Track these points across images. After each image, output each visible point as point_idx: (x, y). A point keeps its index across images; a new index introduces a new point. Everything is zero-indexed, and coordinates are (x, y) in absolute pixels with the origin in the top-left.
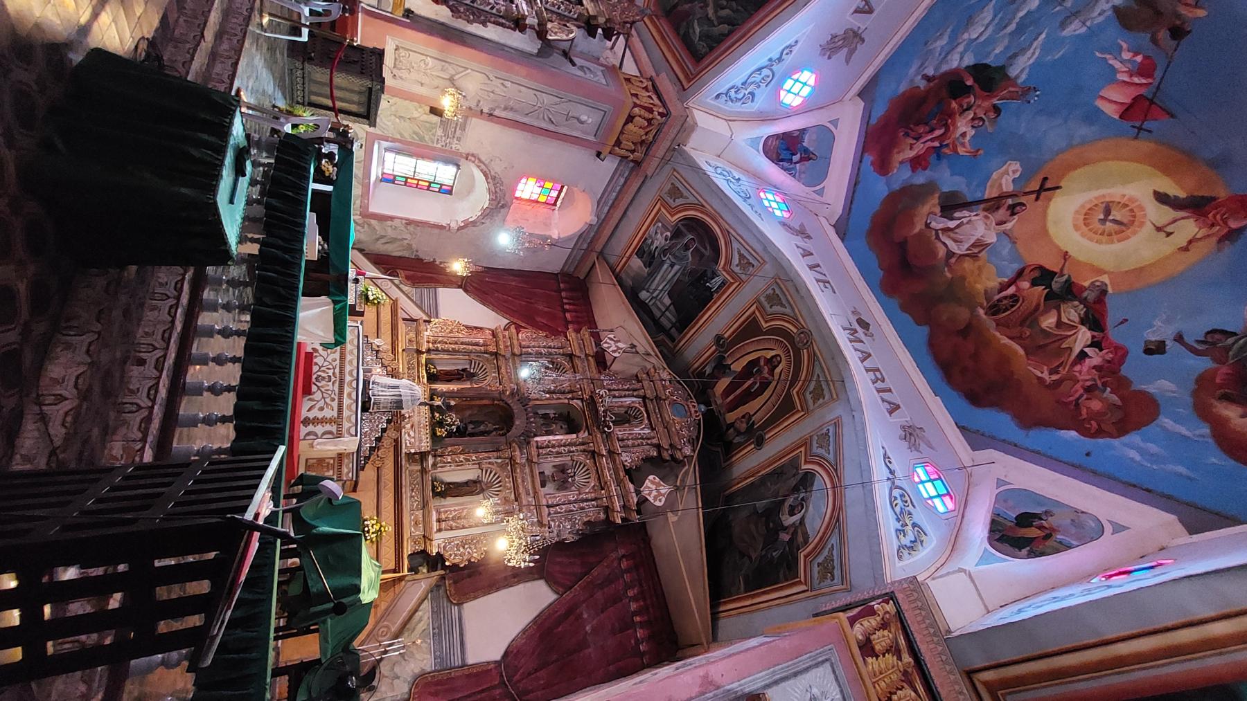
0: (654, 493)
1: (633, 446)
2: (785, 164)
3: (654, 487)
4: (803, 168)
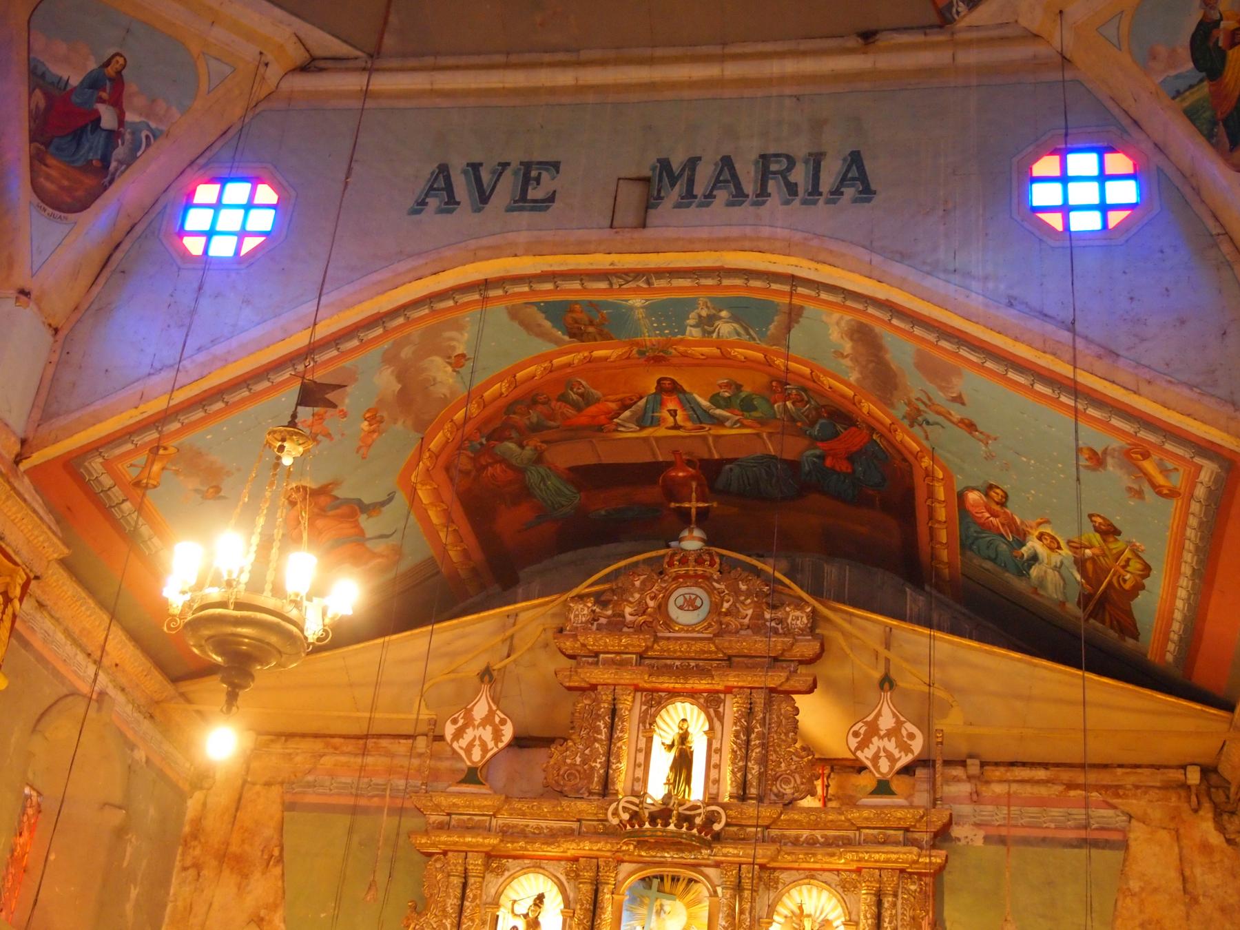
0: (891, 745)
2: (120, 152)
4: (139, 101)
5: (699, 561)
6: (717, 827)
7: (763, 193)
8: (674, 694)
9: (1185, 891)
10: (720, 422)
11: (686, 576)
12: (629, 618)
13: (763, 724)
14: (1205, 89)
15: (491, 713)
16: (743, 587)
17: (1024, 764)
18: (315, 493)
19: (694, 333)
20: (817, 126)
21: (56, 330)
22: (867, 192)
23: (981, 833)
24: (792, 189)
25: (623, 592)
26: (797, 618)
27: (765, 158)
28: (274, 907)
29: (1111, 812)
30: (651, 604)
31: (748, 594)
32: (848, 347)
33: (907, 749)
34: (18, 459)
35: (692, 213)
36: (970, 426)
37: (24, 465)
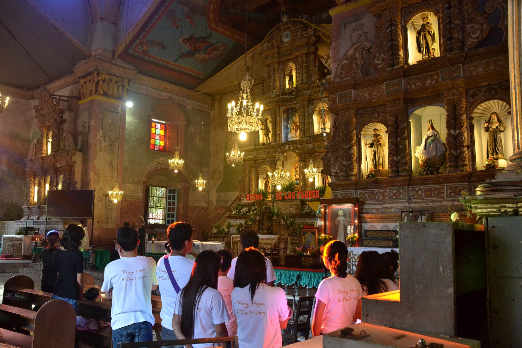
5: (287, 24)
8: (289, 60)
11: (285, 29)
13: (306, 62)
15: (249, 78)
18: (188, 40)
21: (115, 24)
26: (310, 31)
34: (113, 56)
37: (116, 57)
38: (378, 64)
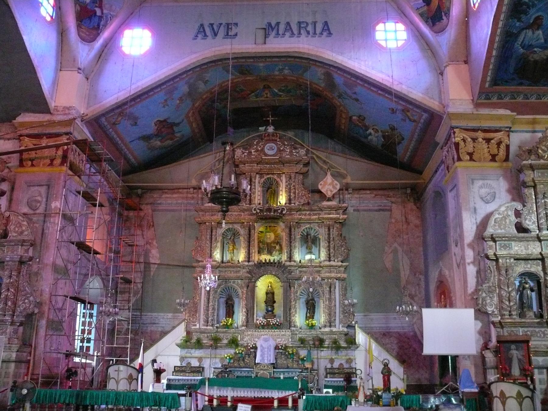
0: (331, 187)
1: (295, 193)
2: (102, 23)
3: (327, 187)
4: (107, 6)
5: (273, 135)
6: (284, 212)
7: (300, 33)
9: (406, 222)
10: (280, 96)
12: (253, 153)
14: (426, 8)
16: (286, 143)
17: (364, 189)
19: (277, 73)
20: (314, 13)
22: (330, 34)
23: (353, 209)
24: (308, 33)
25: (251, 145)
27: (299, 23)
28: (153, 239)
29: (386, 201)
30: (259, 149)
31: (288, 145)
32: (323, 77)
33: (335, 188)
35: (279, 39)
36: (357, 100)
38: (528, 225)
